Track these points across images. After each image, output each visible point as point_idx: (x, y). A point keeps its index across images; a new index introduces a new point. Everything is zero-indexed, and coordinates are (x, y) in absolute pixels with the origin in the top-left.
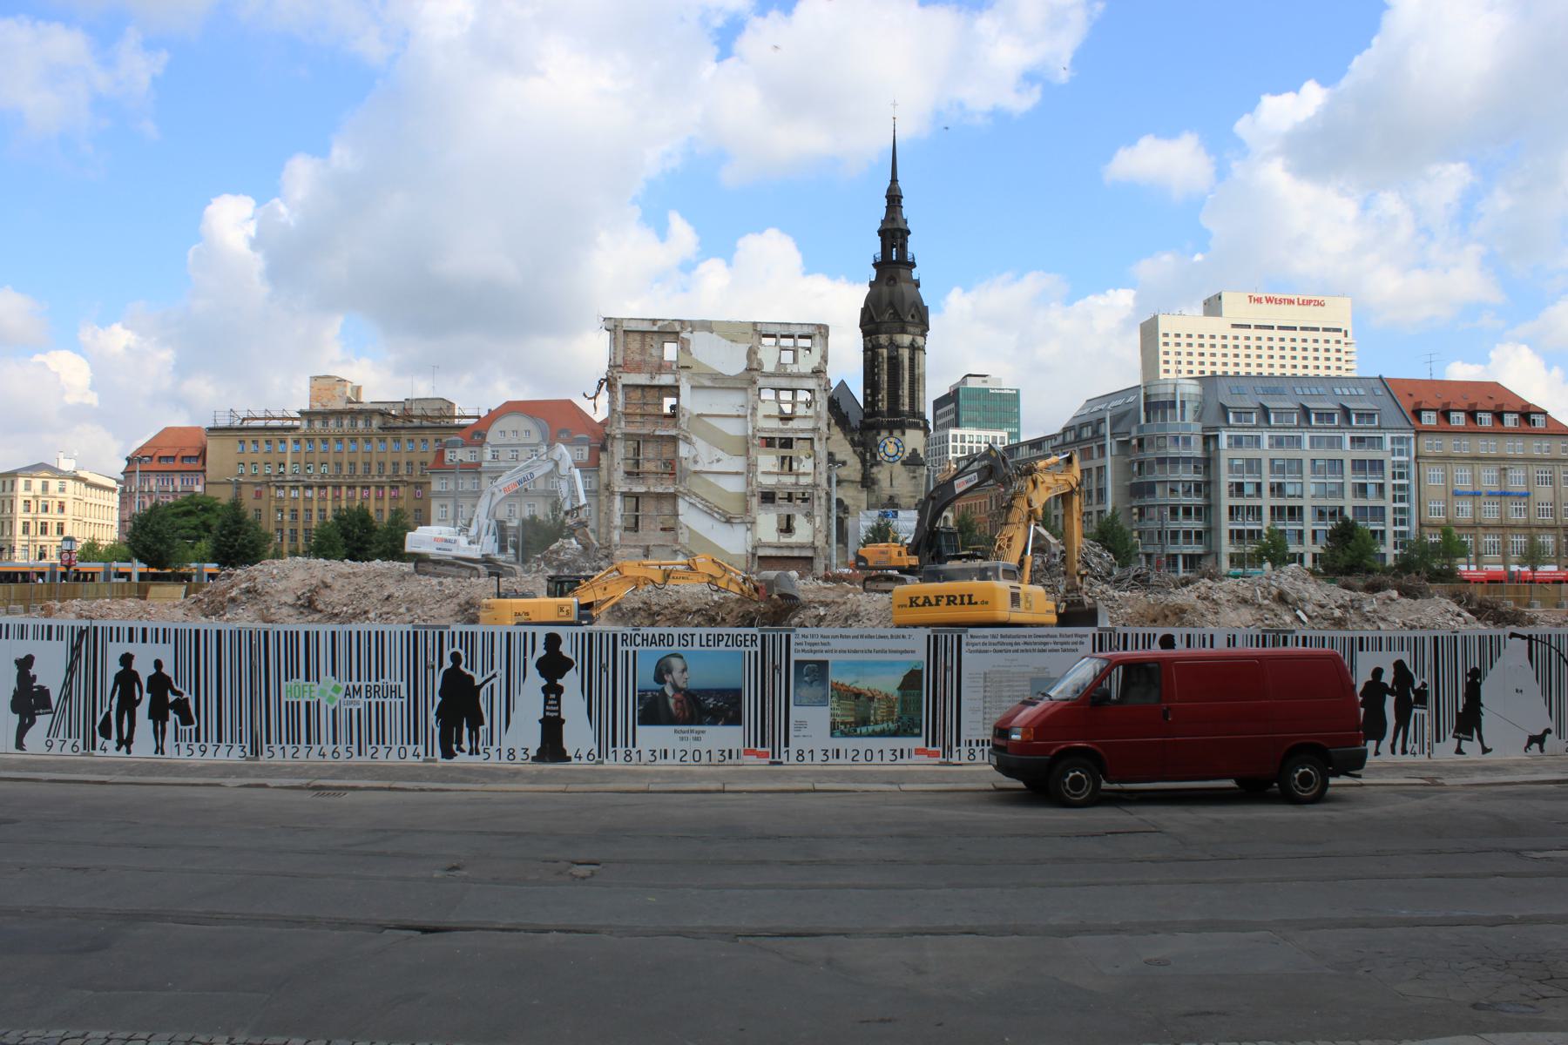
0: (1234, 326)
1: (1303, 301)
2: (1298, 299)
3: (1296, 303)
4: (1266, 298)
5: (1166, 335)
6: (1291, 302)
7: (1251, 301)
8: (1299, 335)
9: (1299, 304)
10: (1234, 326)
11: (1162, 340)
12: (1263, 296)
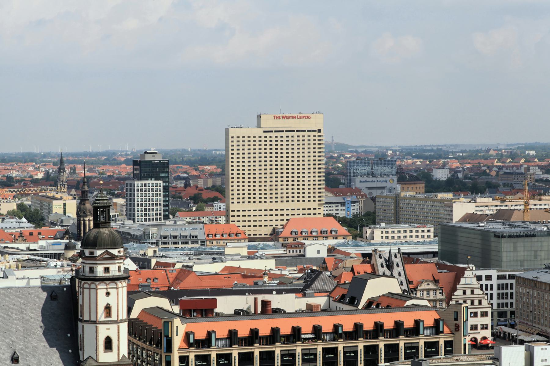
0: (265, 132)
1: (300, 117)
2: (298, 116)
3: (297, 118)
4: (282, 116)
6: (294, 118)
7: (275, 119)
8: (295, 134)
9: (298, 118)
10: (265, 132)
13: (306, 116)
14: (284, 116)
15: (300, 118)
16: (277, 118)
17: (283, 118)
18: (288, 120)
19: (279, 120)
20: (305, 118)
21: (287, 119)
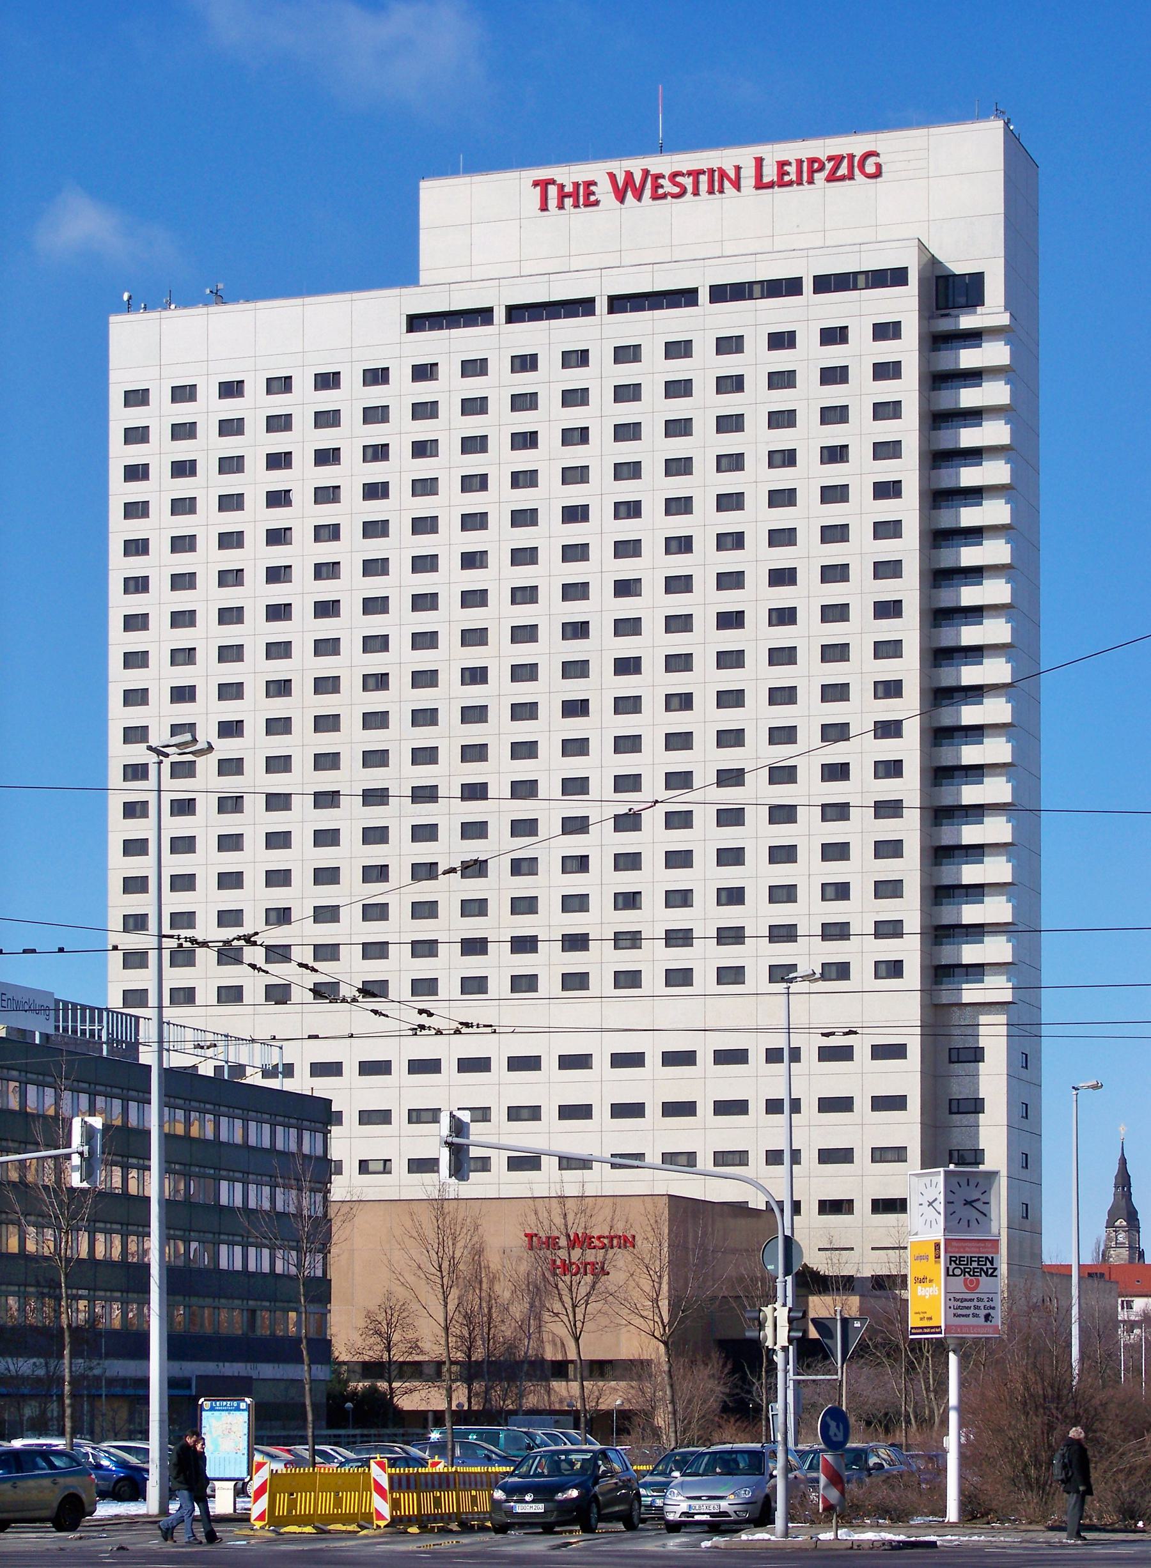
0: (416, 323)
2: (759, 162)
4: (612, 177)
5: (137, 398)
7: (544, 207)
9: (760, 185)
10: (416, 323)
11: (121, 417)
13: (837, 160)
14: (629, 175)
15: (781, 182)
16: (562, 196)
17: (621, 197)
20: (832, 178)
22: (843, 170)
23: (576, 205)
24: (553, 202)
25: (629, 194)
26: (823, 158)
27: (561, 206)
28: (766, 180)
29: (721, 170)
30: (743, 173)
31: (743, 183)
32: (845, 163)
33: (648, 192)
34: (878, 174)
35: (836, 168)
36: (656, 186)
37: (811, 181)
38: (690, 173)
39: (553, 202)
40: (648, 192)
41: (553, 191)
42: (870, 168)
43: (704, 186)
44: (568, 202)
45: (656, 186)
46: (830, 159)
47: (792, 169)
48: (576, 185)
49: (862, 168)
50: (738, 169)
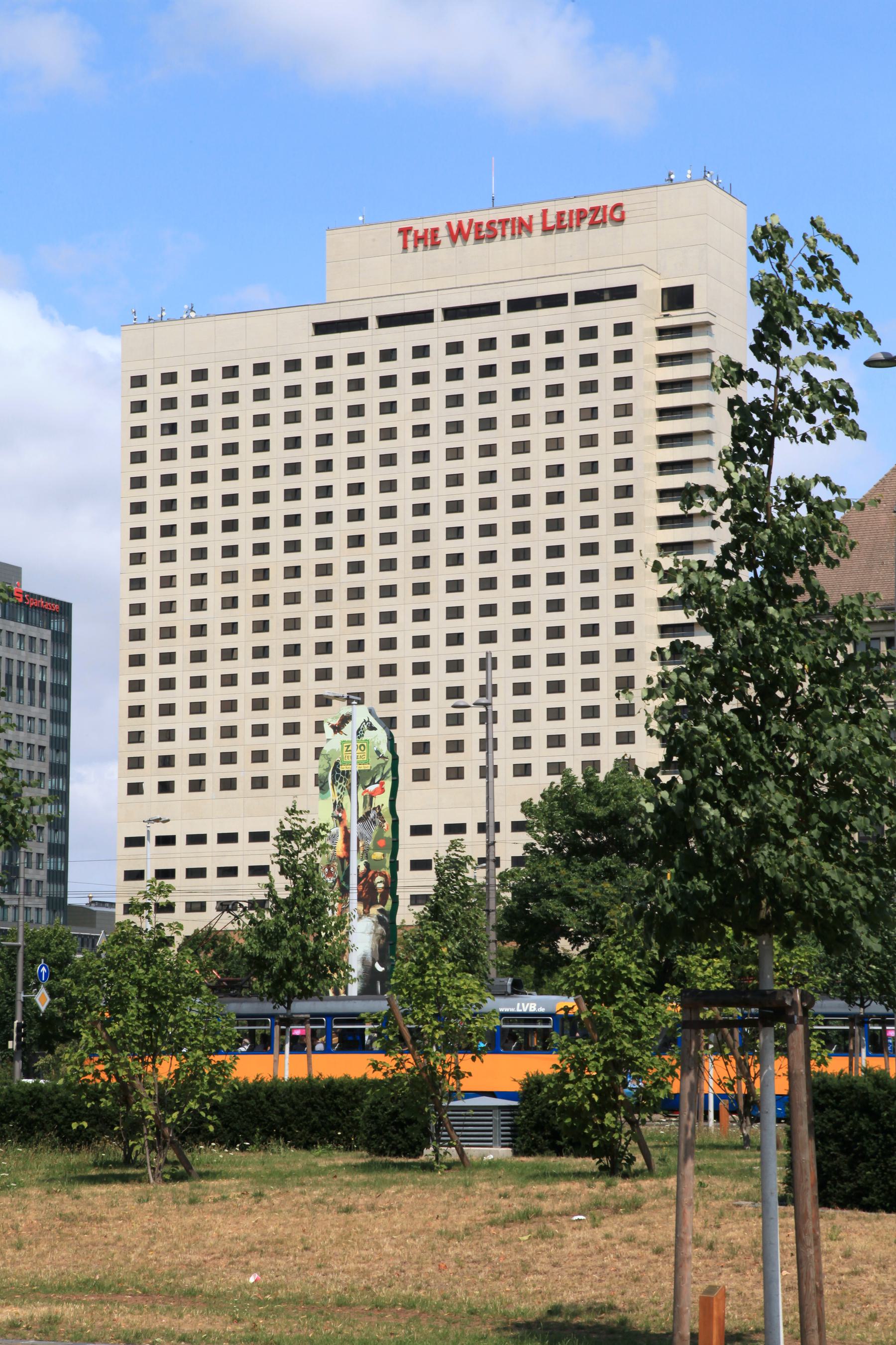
0: (321, 328)
1: (560, 215)
2: (545, 212)
3: (537, 228)
4: (449, 225)
6: (523, 227)
7: (405, 248)
9: (546, 230)
10: (321, 328)
12: (440, 223)
14: (460, 223)
15: (560, 227)
16: (418, 239)
17: (454, 239)
18: (484, 245)
19: (433, 253)
20: (593, 224)
21: (479, 239)
22: (598, 218)
23: (426, 245)
24: (411, 245)
25: (459, 239)
26: (587, 209)
27: (416, 247)
28: (549, 225)
29: (520, 218)
30: (534, 221)
31: (534, 227)
32: (600, 213)
33: (472, 237)
34: (621, 220)
35: (595, 216)
36: (478, 231)
37: (578, 226)
38: (500, 221)
39: (411, 245)
40: (472, 237)
41: (411, 237)
42: (617, 215)
43: (508, 231)
44: (421, 246)
45: (478, 231)
46: (592, 209)
47: (566, 217)
48: (426, 231)
49: (612, 218)
50: (531, 217)
